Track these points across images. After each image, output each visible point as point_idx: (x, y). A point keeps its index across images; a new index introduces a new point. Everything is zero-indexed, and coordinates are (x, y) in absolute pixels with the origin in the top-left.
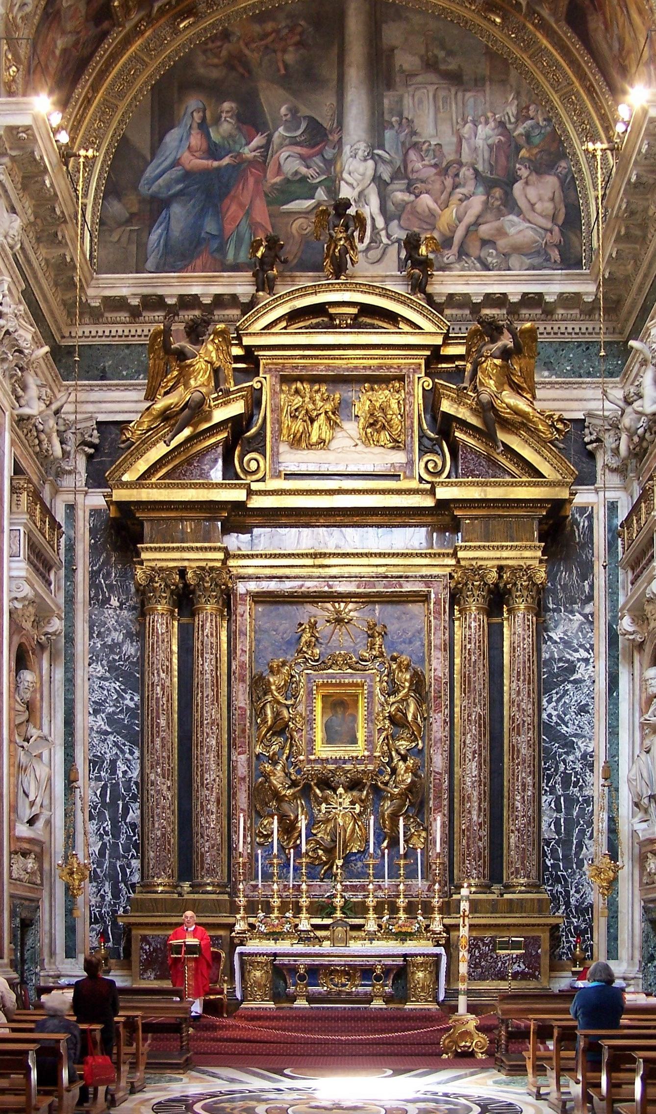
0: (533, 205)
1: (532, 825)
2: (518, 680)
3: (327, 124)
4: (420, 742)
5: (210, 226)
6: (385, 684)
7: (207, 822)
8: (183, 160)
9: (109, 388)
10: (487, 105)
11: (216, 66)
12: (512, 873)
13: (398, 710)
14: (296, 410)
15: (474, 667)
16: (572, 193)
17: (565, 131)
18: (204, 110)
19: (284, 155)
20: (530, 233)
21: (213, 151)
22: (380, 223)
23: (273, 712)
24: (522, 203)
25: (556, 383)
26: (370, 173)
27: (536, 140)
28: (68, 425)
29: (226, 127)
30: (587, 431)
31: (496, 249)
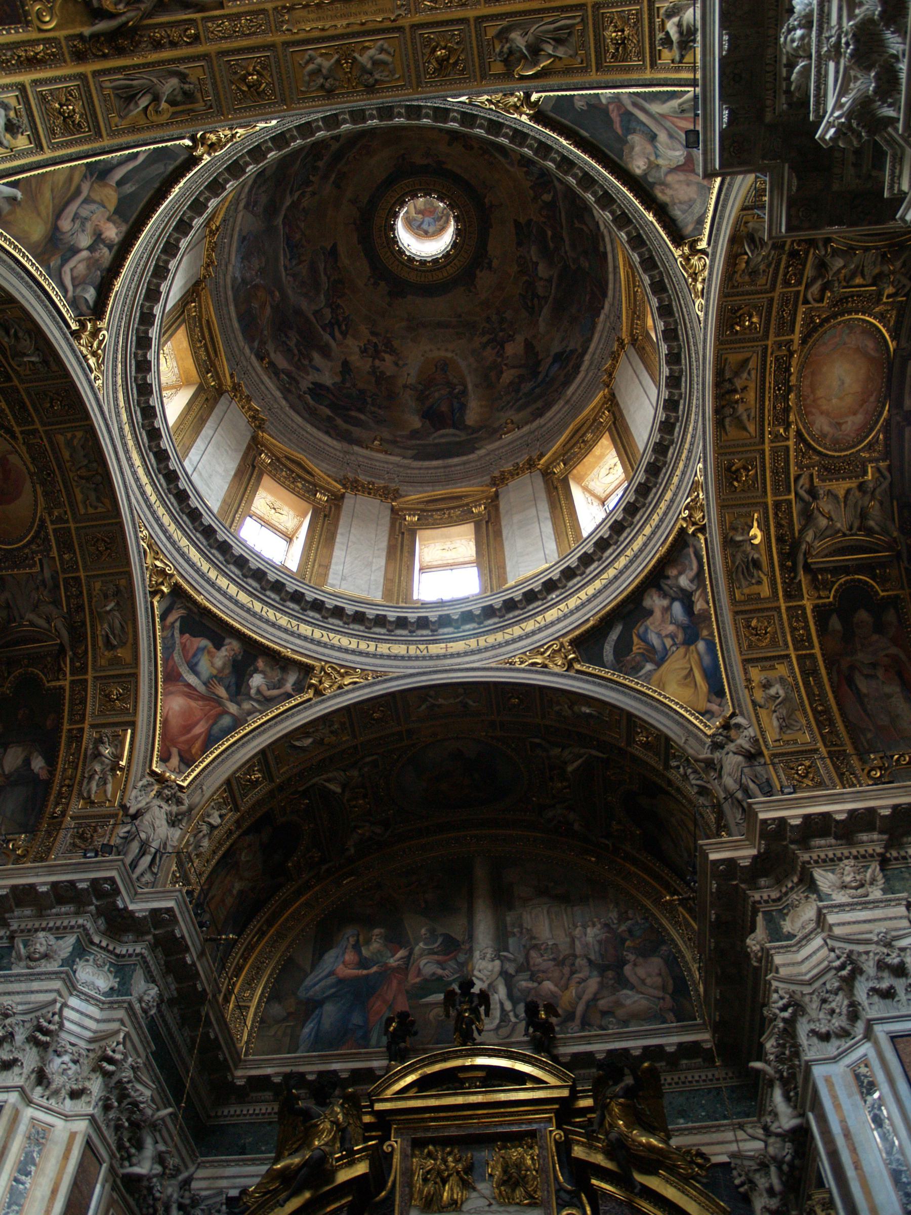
0: (643, 982)
3: (459, 938)
5: (356, 1019)
9: (245, 1162)
14: (428, 1172)
17: (661, 924)
18: (358, 935)
19: (423, 962)
20: (644, 1002)
21: (363, 963)
22: (508, 1006)
24: (633, 979)
30: (735, 1173)
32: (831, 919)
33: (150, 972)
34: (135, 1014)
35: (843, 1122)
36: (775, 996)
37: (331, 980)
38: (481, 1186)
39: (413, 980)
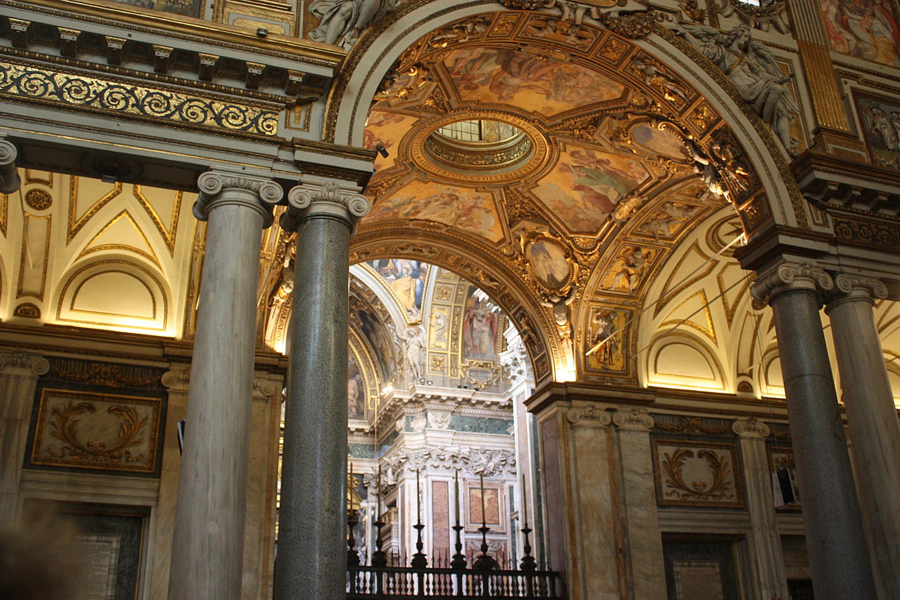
32: (428, 434)
35: (409, 500)
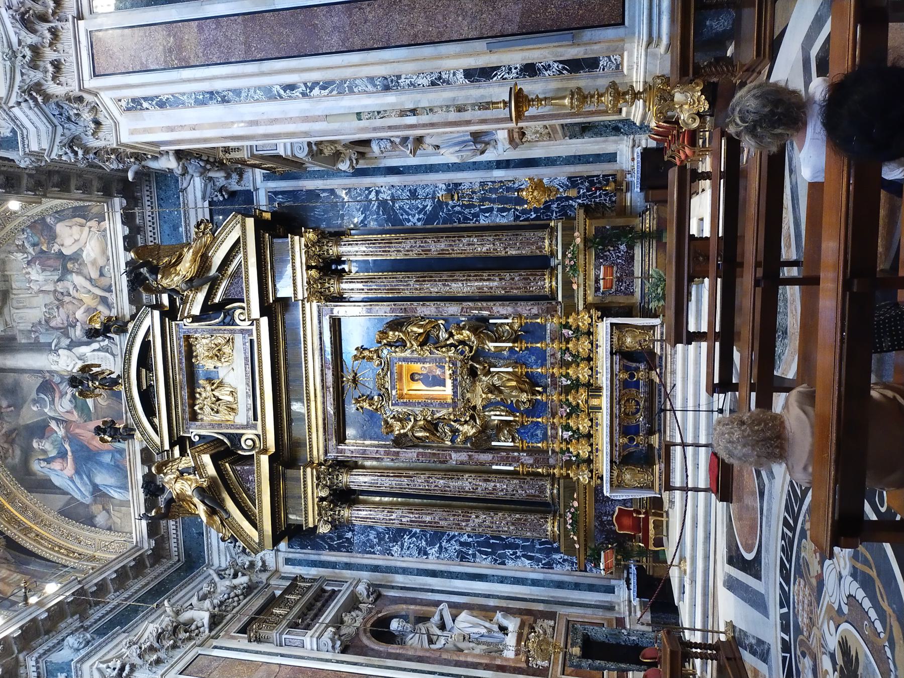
1: (501, 237)
2: (389, 251)
3: (41, 380)
4: (439, 322)
5: (107, 459)
6: (397, 350)
7: (502, 490)
8: (69, 475)
10: (19, 273)
11: (13, 452)
12: (541, 251)
13: (416, 339)
14: (213, 410)
15: (381, 286)
16: (65, 212)
21: (62, 455)
23: (421, 431)
24: (74, 249)
25: (185, 222)
26: (66, 352)
27: (36, 239)
28: (234, 564)
29: (47, 445)
30: (215, 199)
31: (105, 266)
33: (54, 647)
34: (88, 654)
36: (64, 158)
37: (77, 479)
38: (221, 375)
39: (75, 417)
